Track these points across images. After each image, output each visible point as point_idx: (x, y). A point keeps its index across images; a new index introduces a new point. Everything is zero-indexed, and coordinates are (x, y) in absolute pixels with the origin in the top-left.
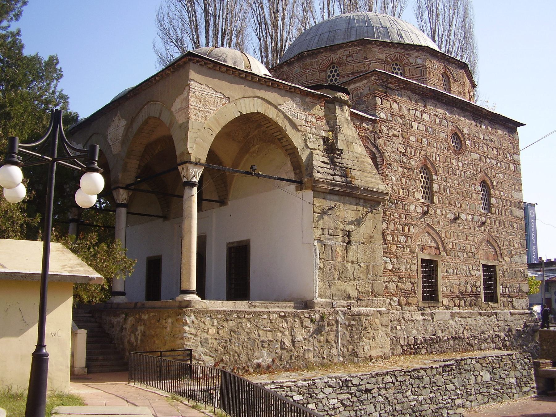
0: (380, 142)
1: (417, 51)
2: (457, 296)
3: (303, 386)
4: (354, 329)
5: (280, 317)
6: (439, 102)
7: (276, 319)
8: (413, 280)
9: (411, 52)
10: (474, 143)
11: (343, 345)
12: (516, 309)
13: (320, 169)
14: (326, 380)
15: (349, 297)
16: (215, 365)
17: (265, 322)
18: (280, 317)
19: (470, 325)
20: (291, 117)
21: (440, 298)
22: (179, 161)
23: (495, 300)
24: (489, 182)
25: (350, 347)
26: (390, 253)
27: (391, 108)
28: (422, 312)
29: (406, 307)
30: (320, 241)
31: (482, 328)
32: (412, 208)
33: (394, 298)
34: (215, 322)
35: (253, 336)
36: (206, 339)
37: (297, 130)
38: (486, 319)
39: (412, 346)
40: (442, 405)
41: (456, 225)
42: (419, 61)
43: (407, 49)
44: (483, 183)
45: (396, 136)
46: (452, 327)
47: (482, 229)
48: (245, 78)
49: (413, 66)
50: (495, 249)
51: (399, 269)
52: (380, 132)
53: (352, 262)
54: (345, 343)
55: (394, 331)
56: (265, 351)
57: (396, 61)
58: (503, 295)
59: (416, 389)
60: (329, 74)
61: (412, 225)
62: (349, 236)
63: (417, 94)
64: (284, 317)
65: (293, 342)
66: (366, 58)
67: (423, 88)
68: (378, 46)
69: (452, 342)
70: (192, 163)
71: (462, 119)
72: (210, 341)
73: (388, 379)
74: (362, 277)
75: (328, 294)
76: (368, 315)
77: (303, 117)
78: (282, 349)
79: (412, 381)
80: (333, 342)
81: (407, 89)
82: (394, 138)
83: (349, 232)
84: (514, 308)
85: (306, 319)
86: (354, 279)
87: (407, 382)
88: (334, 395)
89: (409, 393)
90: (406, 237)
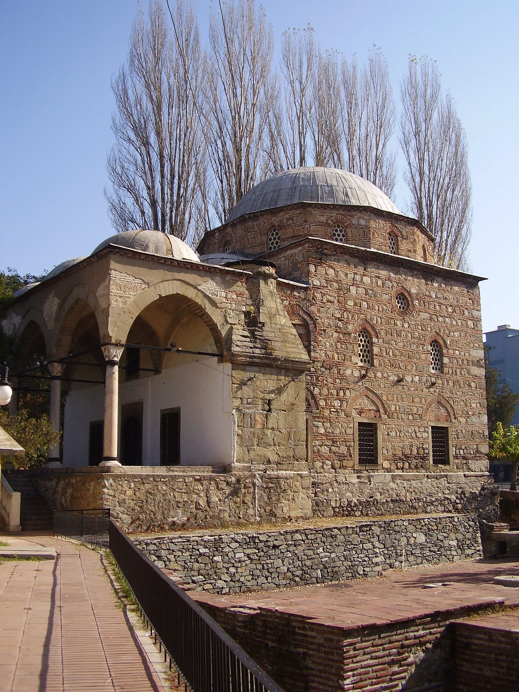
0: (314, 309)
1: (361, 211)
2: (400, 459)
3: (209, 541)
4: (272, 491)
5: (196, 480)
6: (382, 263)
7: (191, 482)
8: (348, 444)
9: (354, 213)
10: (424, 302)
11: (260, 506)
13: (239, 343)
14: (233, 536)
15: (269, 462)
16: (132, 523)
17: (180, 485)
18: (196, 480)
19: (415, 488)
20: (210, 296)
21: (380, 460)
22: (102, 342)
23: (446, 462)
24: (441, 342)
25: (268, 508)
26: (323, 418)
27: (326, 273)
28: (359, 474)
29: (340, 470)
30: (238, 409)
31: (429, 490)
32: (348, 372)
33: (327, 462)
34: (133, 485)
35: (168, 497)
36: (124, 500)
37: (217, 307)
39: (345, 508)
40: (357, 563)
41: (400, 388)
42: (362, 222)
43: (349, 211)
44: (435, 343)
45: (331, 302)
46: (392, 489)
47: (432, 390)
48: (164, 264)
49: (356, 228)
50: (447, 410)
51: (333, 433)
52: (313, 299)
53: (273, 429)
54: (262, 504)
55: (325, 493)
56: (180, 511)
57: (338, 223)
58: (456, 457)
59: (329, 547)
60: (271, 236)
61: (348, 389)
62: (269, 404)
63: (356, 257)
65: (208, 503)
66: (306, 221)
67: (363, 251)
68: (318, 208)
69: (391, 505)
70: (113, 344)
71: (410, 278)
72: (127, 501)
73: (298, 536)
74: (283, 442)
75: (246, 459)
76: (287, 479)
77: (224, 294)
78: (197, 509)
79: (324, 539)
80: (250, 503)
81: (345, 253)
82: (330, 304)
83: (269, 400)
84: (469, 469)
85: (221, 482)
86: (275, 445)
87: (319, 540)
88: (240, 550)
89: (321, 549)
90: (341, 401)
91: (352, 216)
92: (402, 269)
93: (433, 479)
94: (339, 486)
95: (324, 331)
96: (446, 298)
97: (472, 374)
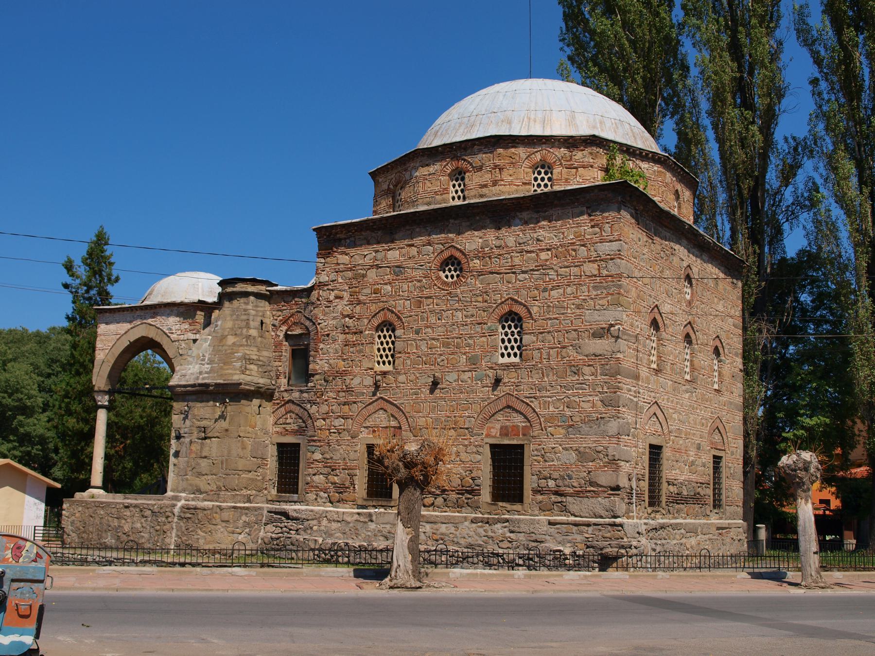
11: (177, 536)
12: (576, 516)
31: (470, 540)
33: (322, 494)
38: (481, 527)
50: (526, 417)
51: (331, 458)
58: (537, 491)
61: (355, 402)
63: (379, 230)
64: (127, 507)
76: (205, 510)
81: (361, 230)
91: (406, 170)
92: (452, 221)
93: (480, 524)
94: (329, 525)
95: (328, 335)
96: (538, 240)
97: (587, 353)
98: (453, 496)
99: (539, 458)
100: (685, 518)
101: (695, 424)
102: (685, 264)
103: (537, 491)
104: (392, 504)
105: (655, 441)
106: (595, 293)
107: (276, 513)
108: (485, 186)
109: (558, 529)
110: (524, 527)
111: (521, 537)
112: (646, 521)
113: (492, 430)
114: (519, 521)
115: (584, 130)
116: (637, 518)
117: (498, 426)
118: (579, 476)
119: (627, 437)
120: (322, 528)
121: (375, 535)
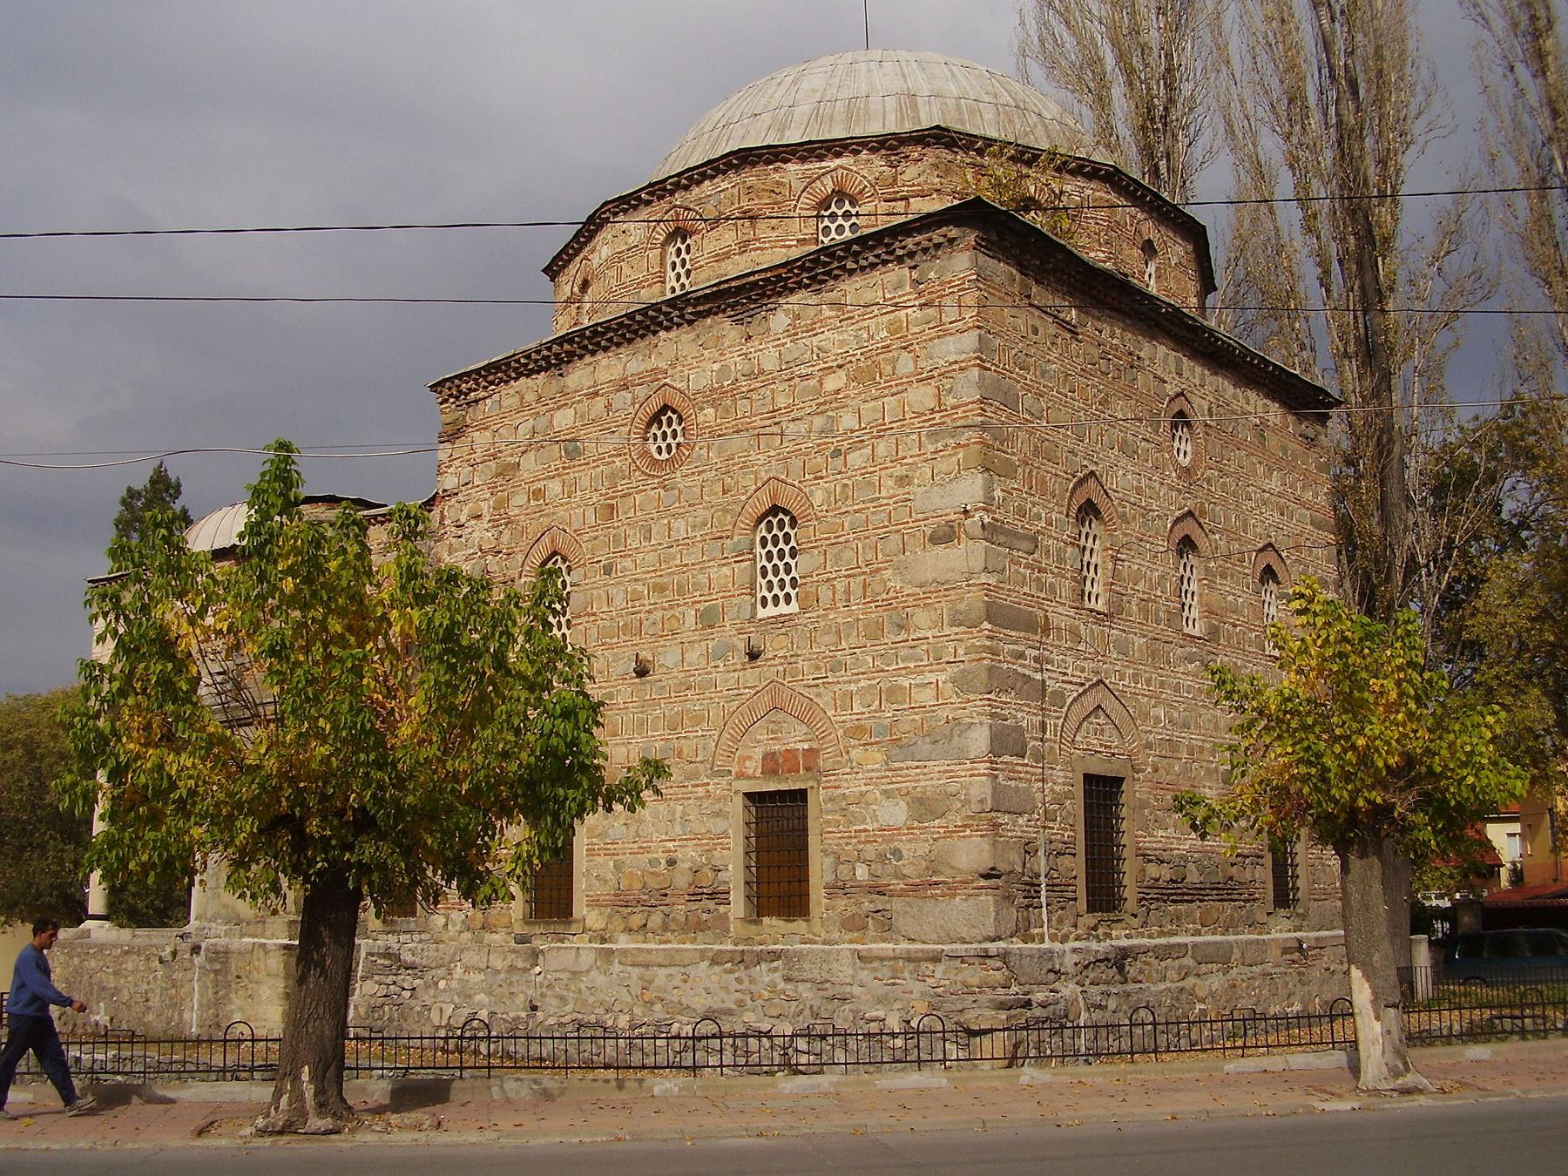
21: (580, 908)
38: (731, 971)
58: (837, 889)
98: (680, 910)
99: (837, 817)
100: (1197, 933)
101: (1216, 728)
102: (1171, 389)
103: (837, 889)
104: (574, 928)
105: (1097, 768)
106: (931, 448)
107: (381, 956)
108: (727, 256)
109: (875, 970)
110: (810, 970)
111: (805, 991)
112: (1077, 944)
113: (748, 763)
114: (800, 955)
115: (928, 118)
116: (1053, 938)
117: (758, 754)
118: (914, 851)
119: (1015, 760)
120: (454, 984)
121: (543, 995)
